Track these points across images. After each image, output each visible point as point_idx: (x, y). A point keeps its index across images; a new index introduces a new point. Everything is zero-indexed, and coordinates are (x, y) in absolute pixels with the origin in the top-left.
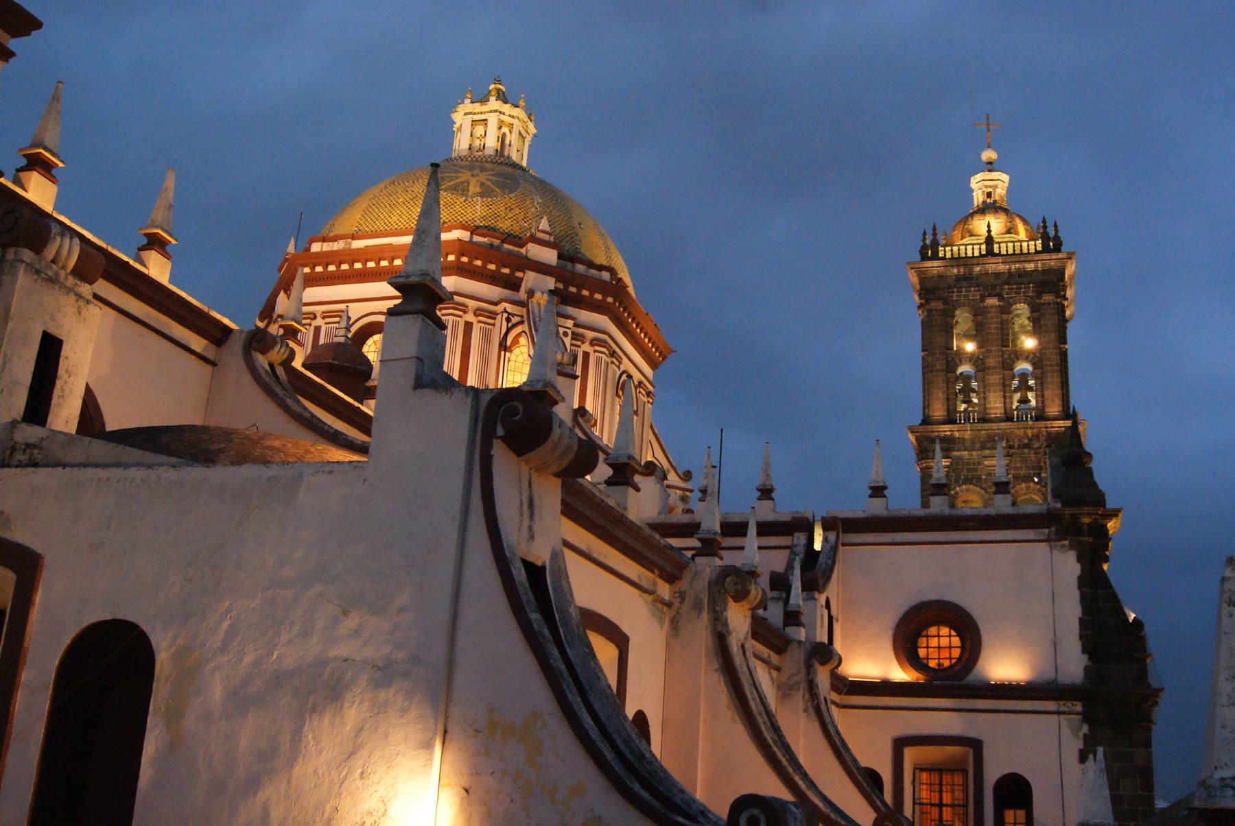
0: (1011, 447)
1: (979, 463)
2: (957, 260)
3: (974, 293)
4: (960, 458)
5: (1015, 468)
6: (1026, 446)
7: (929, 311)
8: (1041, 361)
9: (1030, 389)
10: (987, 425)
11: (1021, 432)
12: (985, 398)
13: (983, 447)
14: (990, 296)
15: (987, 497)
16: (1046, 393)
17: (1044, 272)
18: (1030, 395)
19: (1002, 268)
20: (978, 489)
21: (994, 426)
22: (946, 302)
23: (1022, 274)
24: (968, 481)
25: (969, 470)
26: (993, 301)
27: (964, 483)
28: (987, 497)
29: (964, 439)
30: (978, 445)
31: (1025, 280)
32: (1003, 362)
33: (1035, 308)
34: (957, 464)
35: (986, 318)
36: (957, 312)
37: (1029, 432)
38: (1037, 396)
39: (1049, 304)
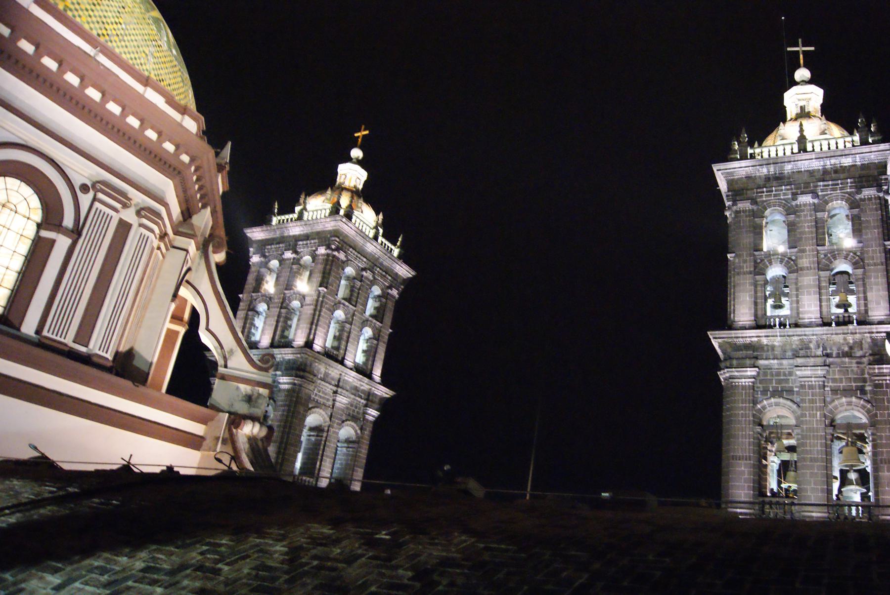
0: (828, 355)
1: (791, 374)
2: (769, 162)
3: (785, 192)
5: (834, 380)
8: (862, 260)
9: (852, 292)
10: (799, 330)
11: (839, 339)
12: (798, 302)
13: (796, 356)
14: (802, 193)
15: (799, 412)
16: (869, 295)
18: (852, 299)
19: (816, 165)
20: (789, 403)
21: (808, 331)
22: (754, 202)
23: (838, 172)
24: (777, 393)
25: (779, 382)
26: (806, 199)
28: (799, 412)
29: (773, 348)
30: (789, 354)
31: (842, 176)
32: (818, 263)
33: (853, 204)
34: (765, 374)
35: (799, 216)
36: (767, 212)
37: (850, 339)
38: (858, 299)
39: (870, 199)
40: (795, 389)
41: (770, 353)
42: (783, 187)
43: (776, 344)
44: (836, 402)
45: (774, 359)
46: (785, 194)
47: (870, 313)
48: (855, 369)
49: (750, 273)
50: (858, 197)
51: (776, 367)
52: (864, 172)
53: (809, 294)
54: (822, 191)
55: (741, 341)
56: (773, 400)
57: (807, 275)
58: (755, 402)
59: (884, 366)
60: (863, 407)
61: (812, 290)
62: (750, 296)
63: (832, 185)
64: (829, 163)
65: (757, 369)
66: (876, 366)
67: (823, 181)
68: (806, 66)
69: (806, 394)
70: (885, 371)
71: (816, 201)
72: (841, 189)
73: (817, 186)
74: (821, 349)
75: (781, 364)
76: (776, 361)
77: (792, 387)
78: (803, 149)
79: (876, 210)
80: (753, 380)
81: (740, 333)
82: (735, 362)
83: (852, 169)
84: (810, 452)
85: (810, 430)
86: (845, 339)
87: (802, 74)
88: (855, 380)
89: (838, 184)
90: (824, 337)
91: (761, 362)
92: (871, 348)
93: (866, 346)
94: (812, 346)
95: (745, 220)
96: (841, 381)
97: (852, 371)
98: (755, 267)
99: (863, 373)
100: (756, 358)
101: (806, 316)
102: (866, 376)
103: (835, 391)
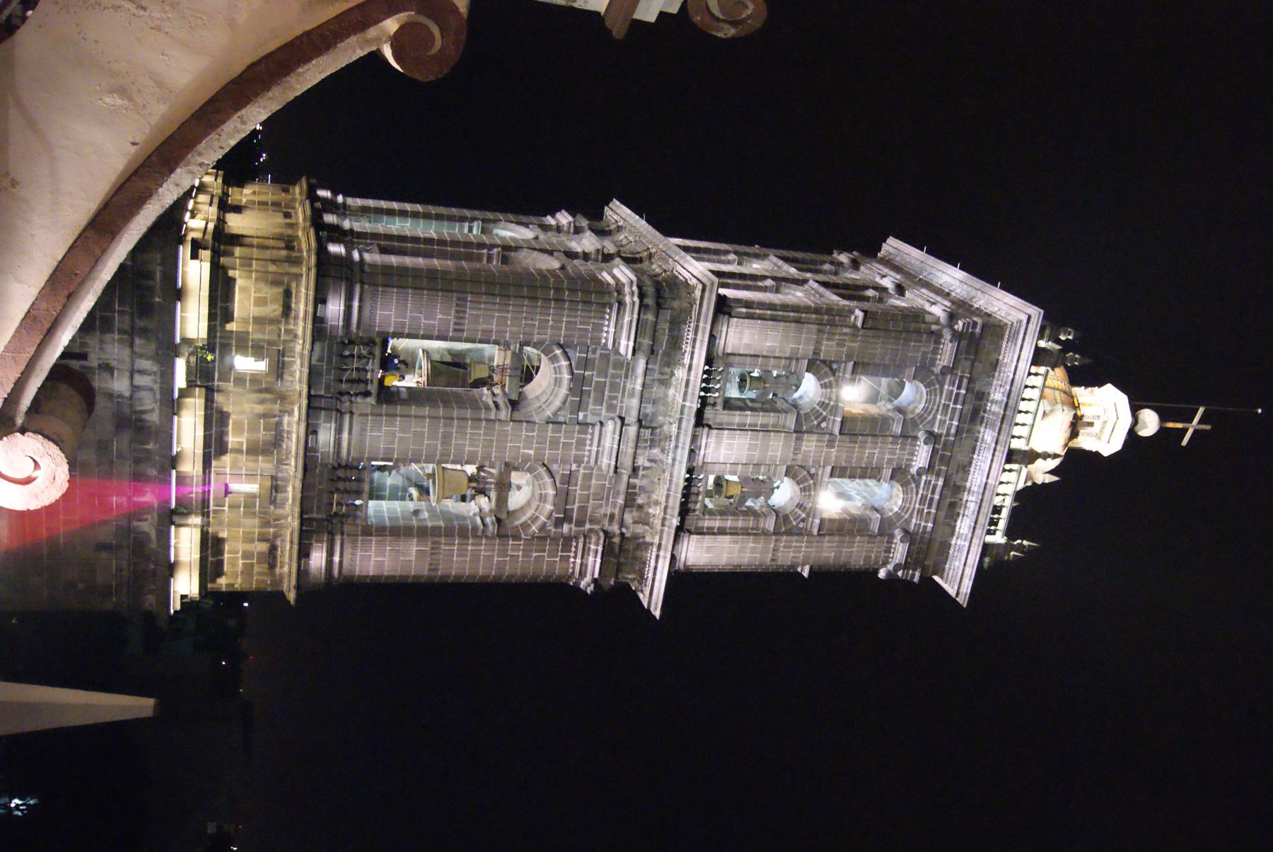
0: (635, 470)
1: (611, 408)
3: (945, 424)
4: (628, 369)
5: (588, 477)
6: (630, 502)
7: (937, 336)
11: (660, 494)
14: (934, 451)
16: (727, 538)
17: (945, 546)
20: (558, 403)
22: (945, 371)
24: (578, 386)
25: (600, 388)
26: (922, 456)
29: (665, 383)
30: (649, 409)
31: (942, 514)
37: (656, 511)
39: (888, 551)
40: (581, 415)
41: (657, 376)
42: (955, 423)
43: (671, 392)
44: (548, 480)
45: (643, 386)
46: (942, 423)
47: (694, 537)
48: (602, 511)
49: (816, 353)
50: (898, 534)
51: (629, 386)
52: (936, 546)
53: (752, 448)
54: (928, 483)
56: (566, 376)
57: (786, 446)
59: (599, 560)
60: (534, 519)
61: (757, 454)
62: (772, 349)
63: (932, 499)
65: (629, 356)
66: (600, 549)
67: (944, 486)
68: (1162, 431)
69: (569, 434)
70: (591, 559)
71: (913, 471)
72: (920, 512)
73: (938, 475)
74: (647, 464)
75: (632, 395)
76: (639, 388)
77: (586, 410)
78: (1012, 456)
79: (867, 558)
80: (610, 346)
81: (705, 326)
82: (650, 317)
83: (947, 530)
84: (462, 433)
85: (503, 437)
86: (657, 503)
87: (1150, 423)
88: (583, 509)
89: (930, 506)
90: (667, 475)
91: (641, 364)
92: (635, 537)
93: (639, 529)
94: (656, 451)
95: (917, 350)
96: (586, 487)
97: (601, 506)
98: (824, 362)
99: (591, 522)
101: (712, 440)
102: (588, 526)
103: (569, 479)
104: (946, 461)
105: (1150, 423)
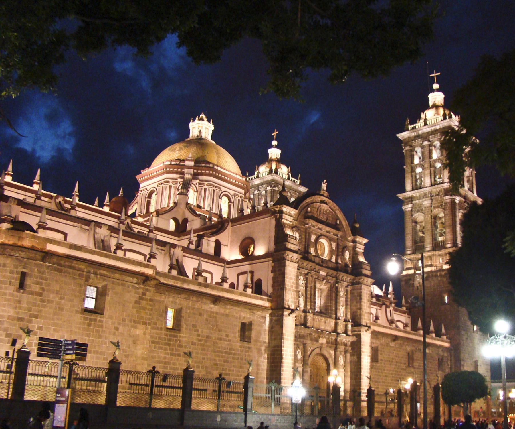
3: (420, 141)
17: (444, 128)
22: (411, 146)
24: (418, 211)
25: (419, 207)
26: (426, 143)
27: (417, 212)
37: (438, 190)
55: (407, 196)
58: (412, 216)
64: (433, 128)
68: (437, 83)
87: (436, 86)
100: (412, 201)
104: (426, 137)
105: (436, 86)
